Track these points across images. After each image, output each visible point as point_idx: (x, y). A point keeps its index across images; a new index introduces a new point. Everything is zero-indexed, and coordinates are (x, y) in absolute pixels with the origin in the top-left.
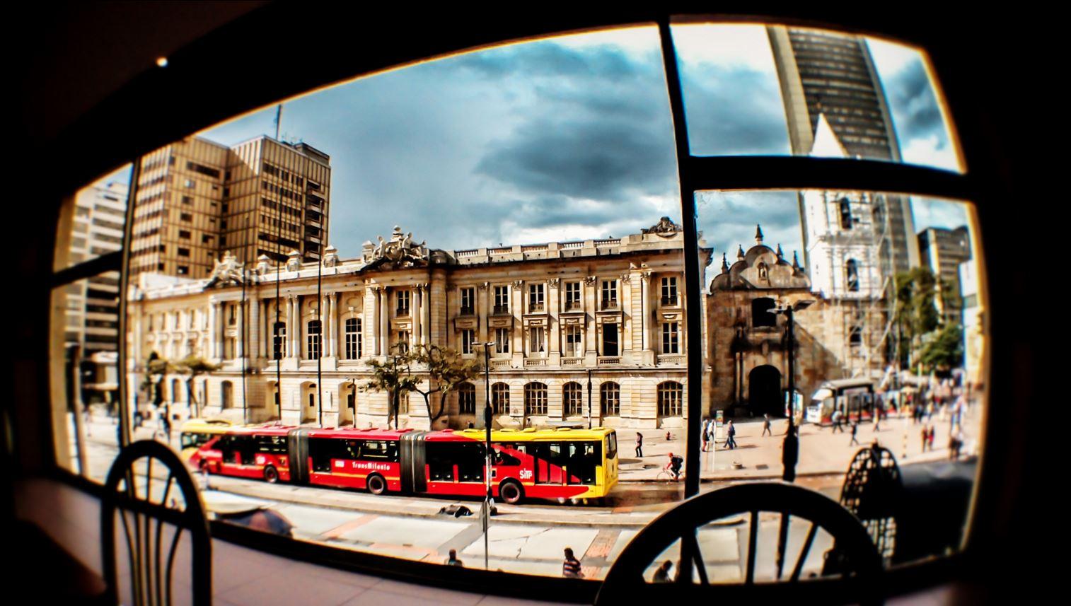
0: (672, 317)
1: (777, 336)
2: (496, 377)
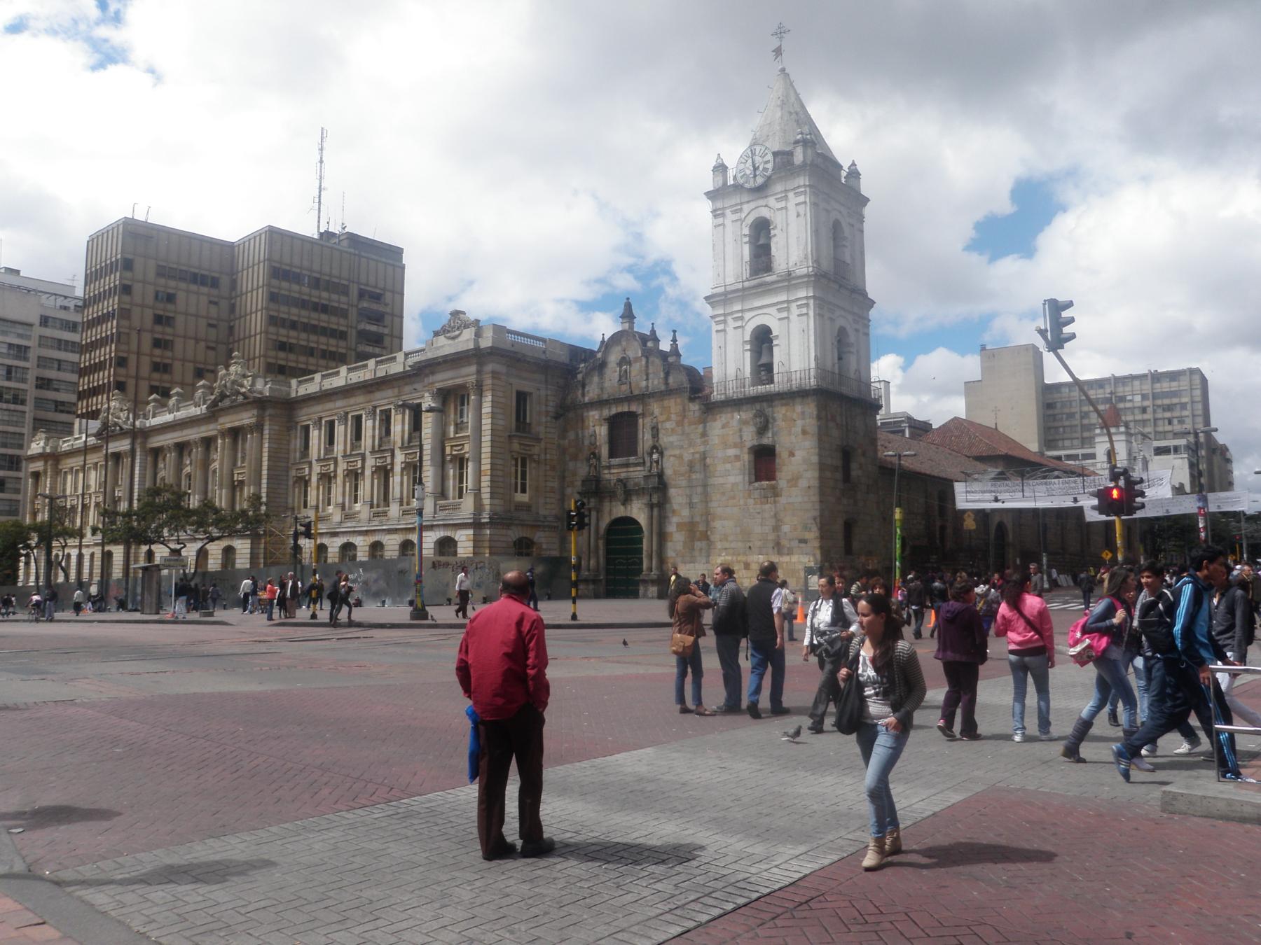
0: (459, 448)
1: (637, 474)
2: (442, 529)
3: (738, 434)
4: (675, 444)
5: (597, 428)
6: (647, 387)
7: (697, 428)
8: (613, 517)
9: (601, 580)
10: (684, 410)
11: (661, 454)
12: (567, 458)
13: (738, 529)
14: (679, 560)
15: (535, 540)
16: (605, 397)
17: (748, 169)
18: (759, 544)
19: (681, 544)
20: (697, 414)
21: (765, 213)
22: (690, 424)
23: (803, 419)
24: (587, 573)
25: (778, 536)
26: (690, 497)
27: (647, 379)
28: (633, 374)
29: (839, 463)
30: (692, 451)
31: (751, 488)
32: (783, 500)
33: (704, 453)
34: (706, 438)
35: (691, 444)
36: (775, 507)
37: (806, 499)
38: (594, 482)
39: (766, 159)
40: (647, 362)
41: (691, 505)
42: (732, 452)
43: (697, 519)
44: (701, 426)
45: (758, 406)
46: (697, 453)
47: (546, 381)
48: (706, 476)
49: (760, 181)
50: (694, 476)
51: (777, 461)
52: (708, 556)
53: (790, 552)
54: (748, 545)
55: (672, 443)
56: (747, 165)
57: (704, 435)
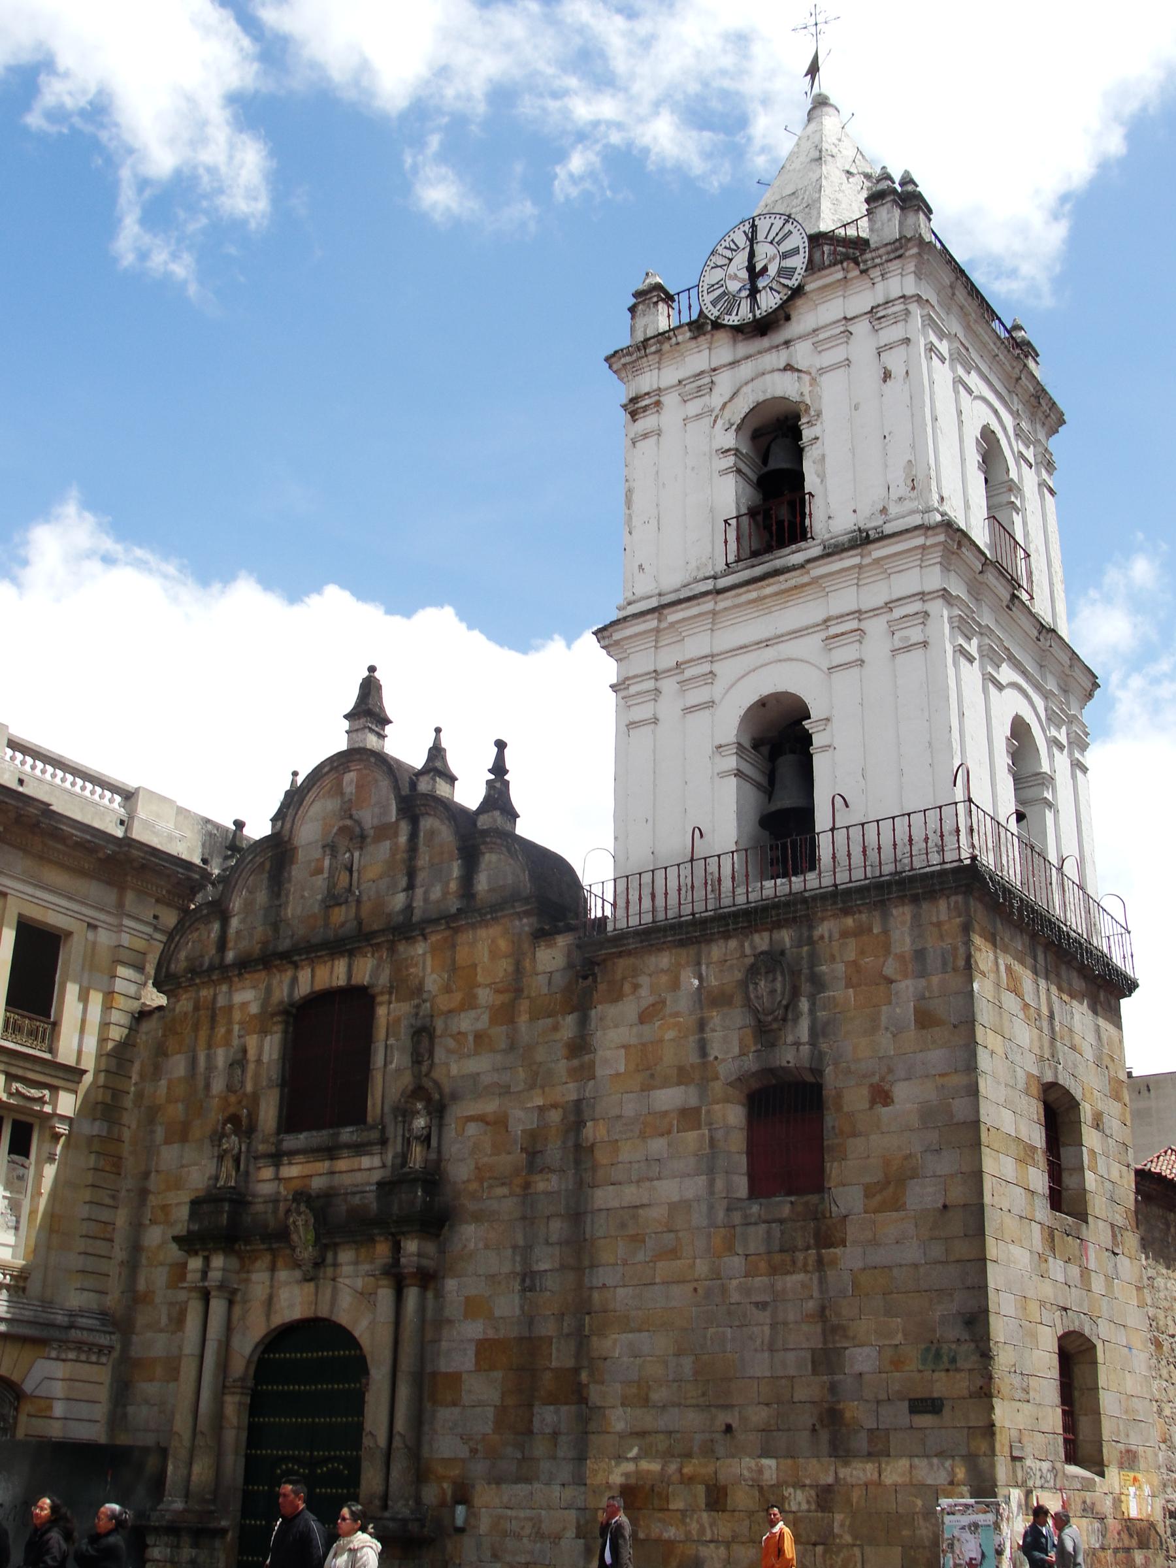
3: (693, 1039)
4: (486, 1079)
5: (252, 1042)
6: (409, 908)
7: (556, 1028)
8: (278, 1320)
9: (223, 1532)
10: (518, 970)
11: (438, 1110)
12: (160, 1133)
13: (687, 1363)
14: (479, 1468)
15: (28, 1387)
16: (285, 945)
17: (735, 277)
18: (759, 1415)
19: (490, 1412)
20: (559, 980)
21: (786, 387)
22: (534, 1018)
23: (922, 974)
24: (179, 1505)
25: (833, 1388)
26: (525, 1251)
27: (410, 887)
28: (372, 873)
29: (1037, 1137)
30: (540, 1102)
31: (737, 1217)
32: (849, 1258)
33: (578, 1103)
34: (587, 1058)
35: (538, 1079)
36: (822, 1281)
37: (937, 1251)
38: (226, 1206)
39: (787, 246)
40: (413, 836)
41: (529, 1280)
42: (669, 1098)
43: (547, 1328)
44: (570, 1020)
45: (761, 941)
46: (555, 1106)
47: (120, 905)
48: (580, 1184)
49: (768, 301)
50: (542, 1184)
51: (830, 1120)
52: (581, 1458)
53: (879, 1451)
54: (723, 1418)
55: (475, 1077)
56: (732, 269)
57: (580, 1046)
